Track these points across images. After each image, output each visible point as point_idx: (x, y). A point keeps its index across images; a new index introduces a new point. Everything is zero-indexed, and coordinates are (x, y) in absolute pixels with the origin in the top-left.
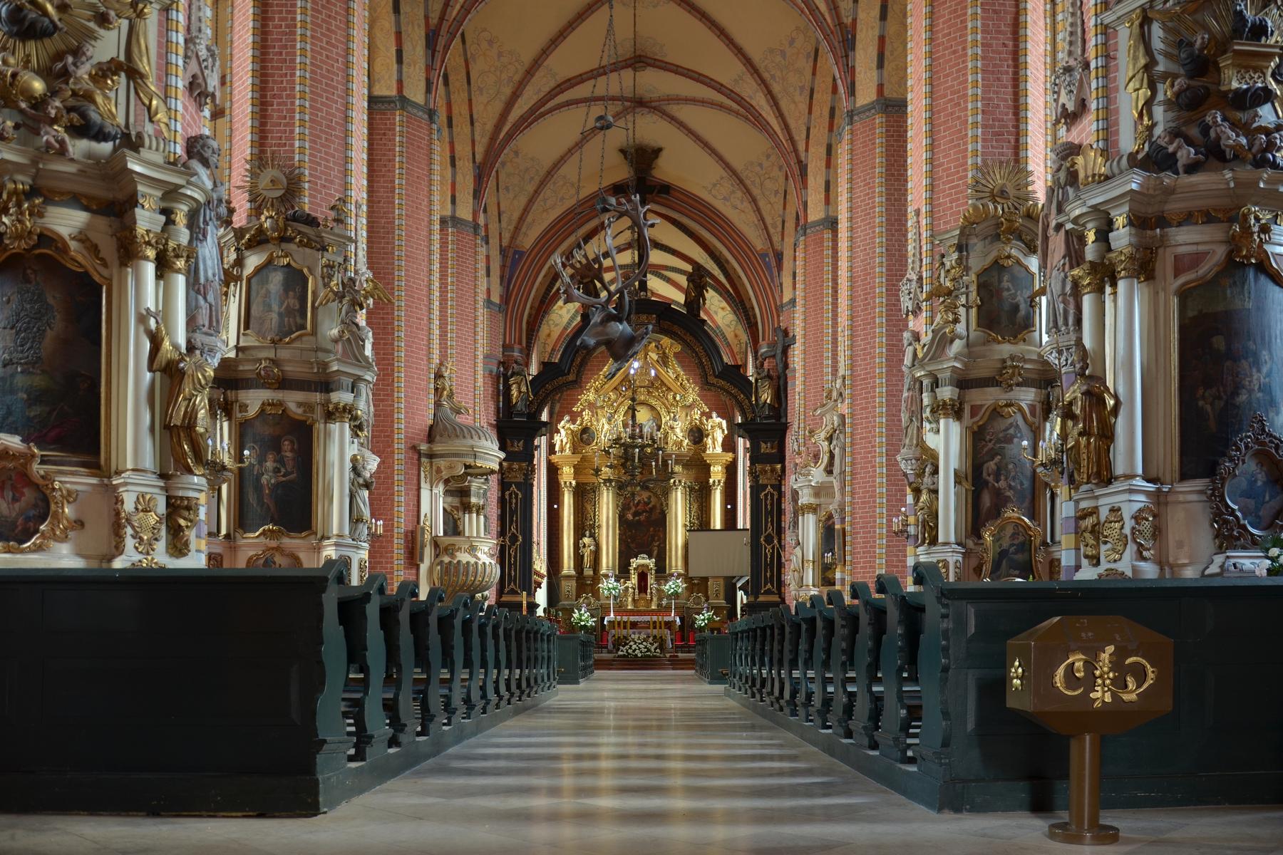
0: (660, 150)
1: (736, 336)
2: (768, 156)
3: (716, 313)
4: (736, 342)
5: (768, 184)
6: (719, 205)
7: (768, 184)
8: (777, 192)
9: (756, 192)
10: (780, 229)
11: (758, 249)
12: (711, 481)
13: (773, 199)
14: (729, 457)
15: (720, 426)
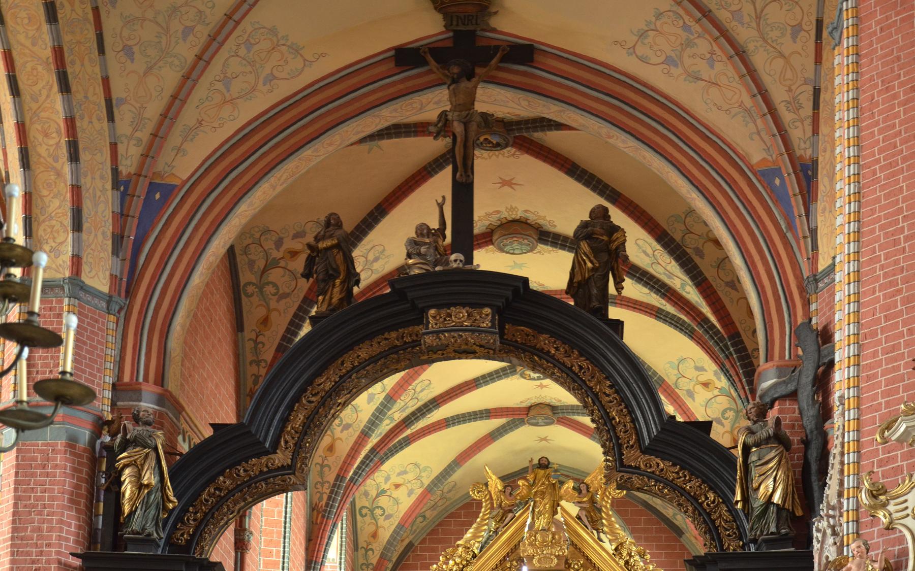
13: (788, 46)
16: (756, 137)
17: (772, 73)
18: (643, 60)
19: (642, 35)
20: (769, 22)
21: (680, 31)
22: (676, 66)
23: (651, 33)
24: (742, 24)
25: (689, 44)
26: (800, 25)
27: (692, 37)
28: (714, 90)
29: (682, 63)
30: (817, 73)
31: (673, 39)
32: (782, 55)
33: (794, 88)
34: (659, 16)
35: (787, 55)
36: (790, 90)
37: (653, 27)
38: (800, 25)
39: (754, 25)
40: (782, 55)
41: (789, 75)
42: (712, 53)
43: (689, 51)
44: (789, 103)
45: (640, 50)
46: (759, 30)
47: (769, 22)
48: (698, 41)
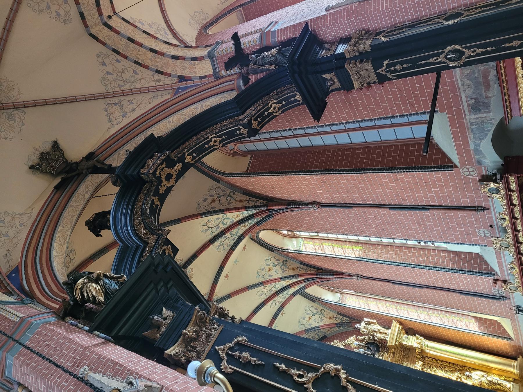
0: (55, 143)
1: (293, 269)
2: (104, 64)
3: (270, 276)
4: (297, 270)
5: (126, 76)
6: (125, 122)
7: (126, 76)
8: (135, 72)
9: (127, 87)
10: (162, 77)
11: (170, 97)
12: (415, 345)
13: (139, 77)
14: (396, 327)
15: (369, 324)
16: (162, 97)
17: (145, 84)
18: (118, 123)
19: (110, 120)
20: (128, 79)
21: (115, 107)
22: (126, 114)
23: (111, 117)
24: (124, 86)
25: (121, 107)
26: (134, 70)
27: (120, 104)
28: (141, 106)
29: (127, 112)
30: (152, 70)
31: (117, 111)
32: (141, 79)
33: (153, 79)
34: (106, 110)
35: (141, 78)
36: (153, 81)
37: (109, 115)
38: (134, 70)
39: (126, 83)
40: (141, 79)
41: (148, 79)
42: (129, 101)
43: (124, 108)
44: (157, 82)
45: (115, 123)
46: (129, 83)
47: (128, 79)
48: (122, 103)
